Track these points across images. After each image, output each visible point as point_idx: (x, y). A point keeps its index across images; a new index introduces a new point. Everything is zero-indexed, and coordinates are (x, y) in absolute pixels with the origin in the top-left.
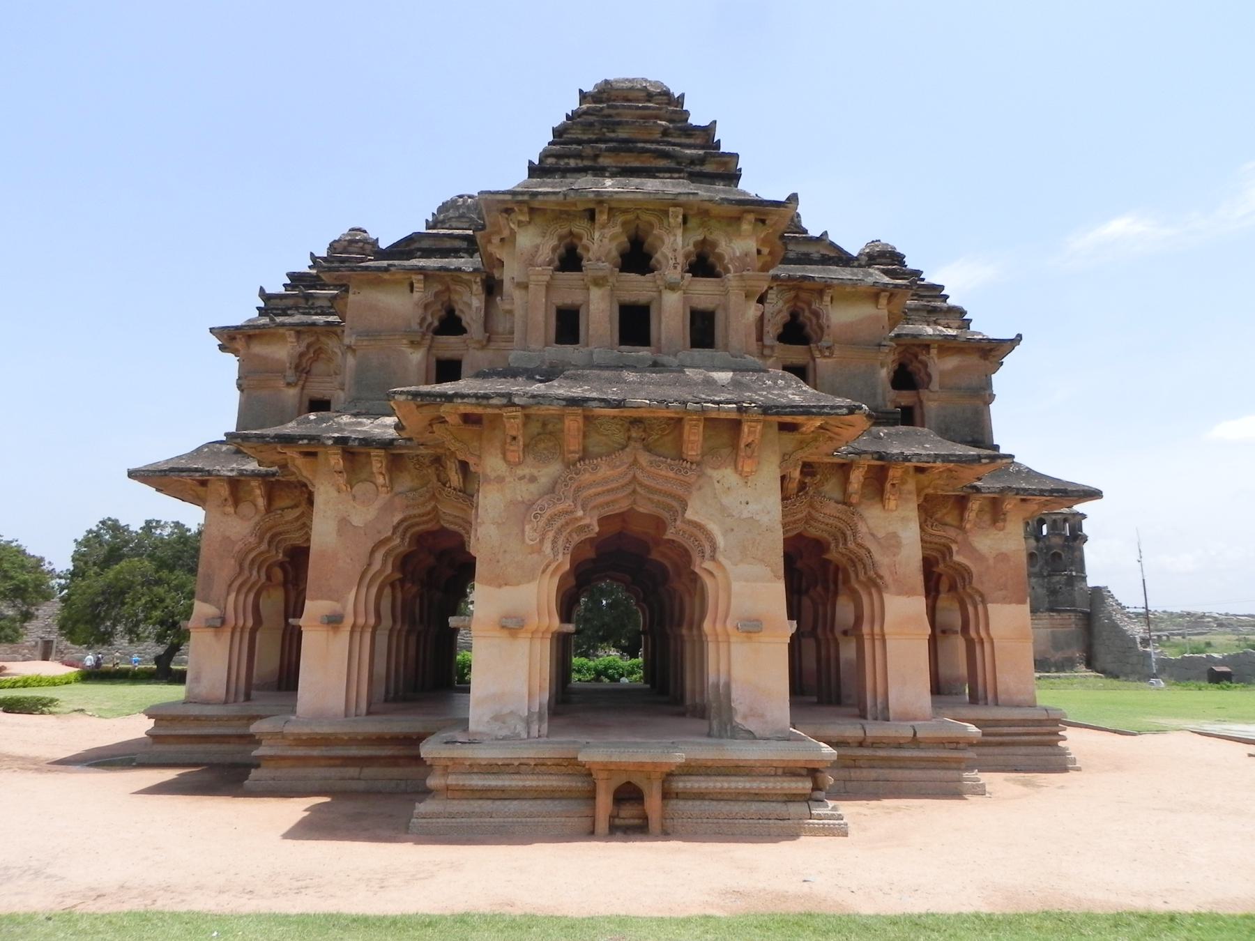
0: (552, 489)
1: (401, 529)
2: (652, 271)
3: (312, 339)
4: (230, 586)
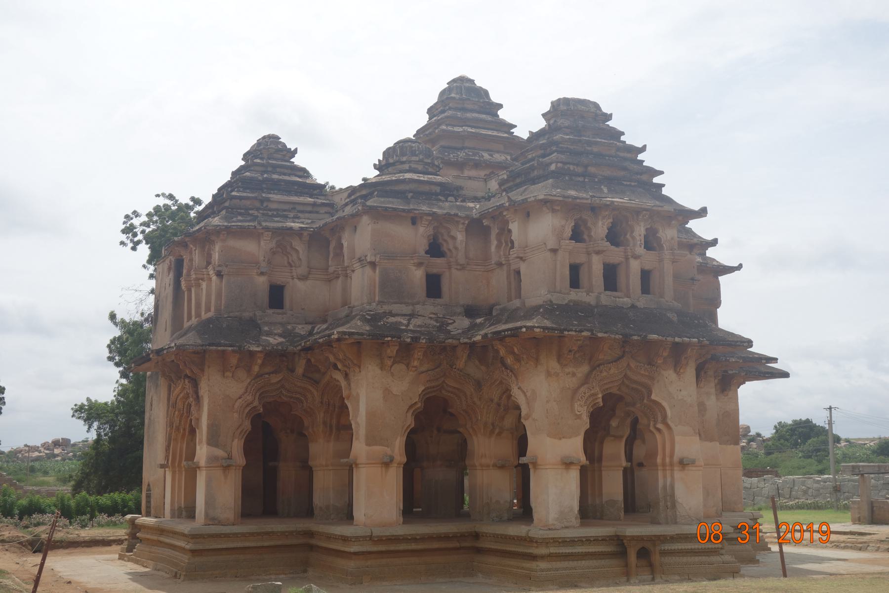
0: (586, 380)
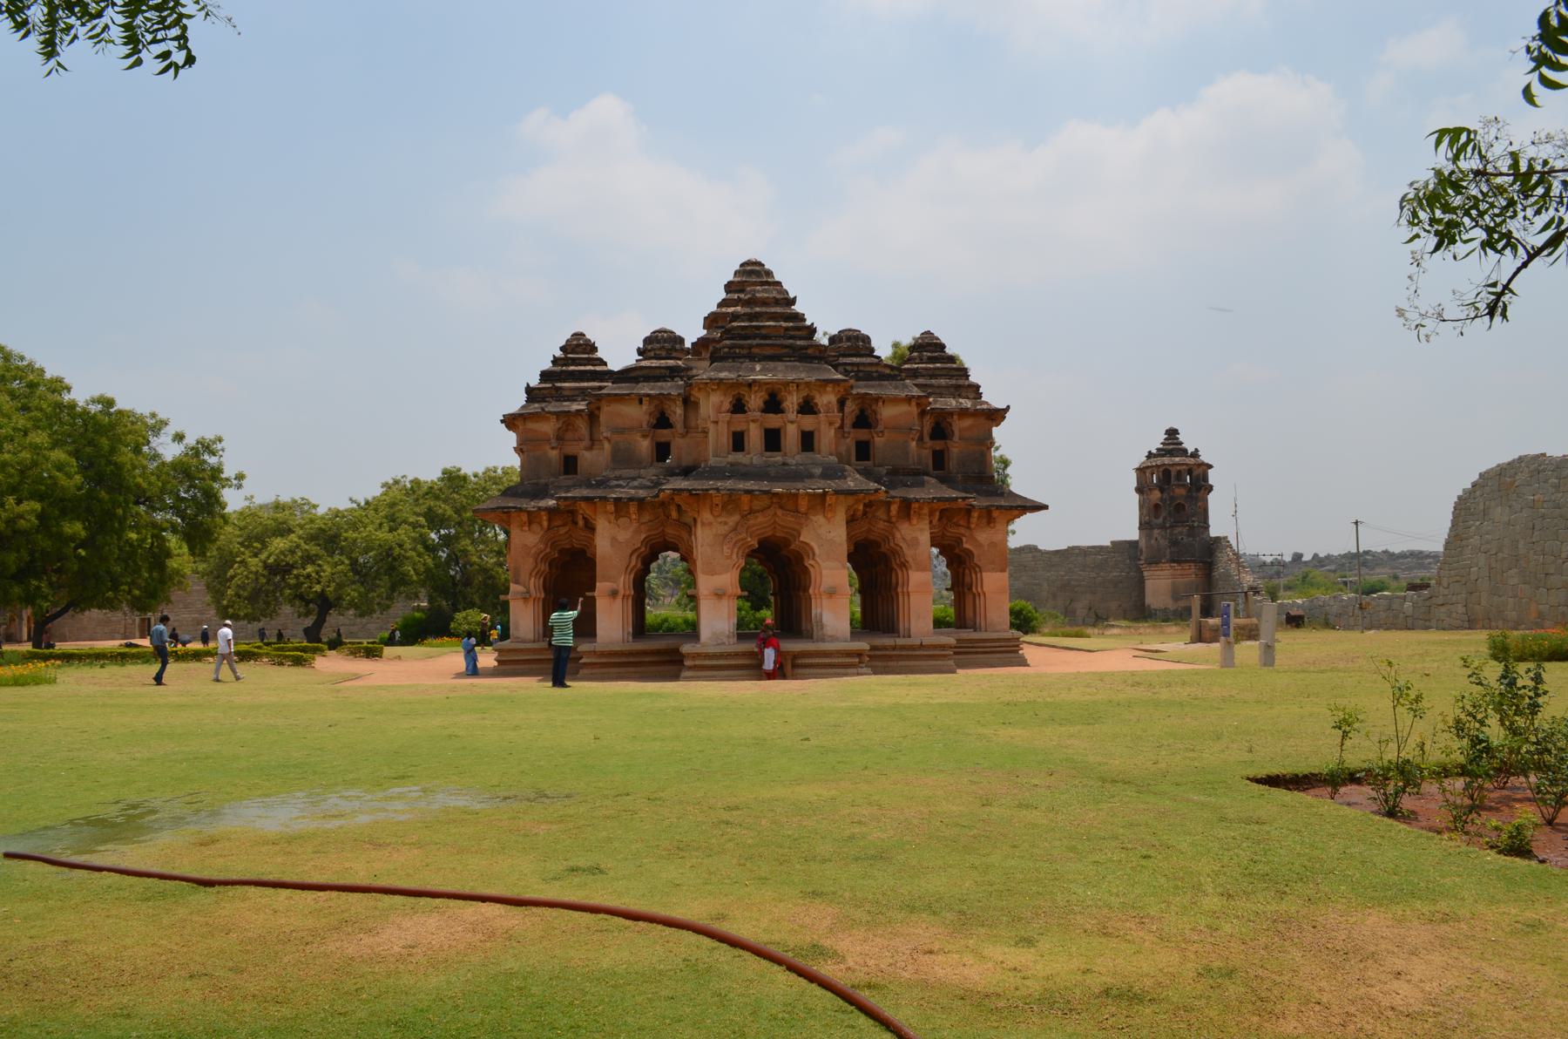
2: (782, 412)
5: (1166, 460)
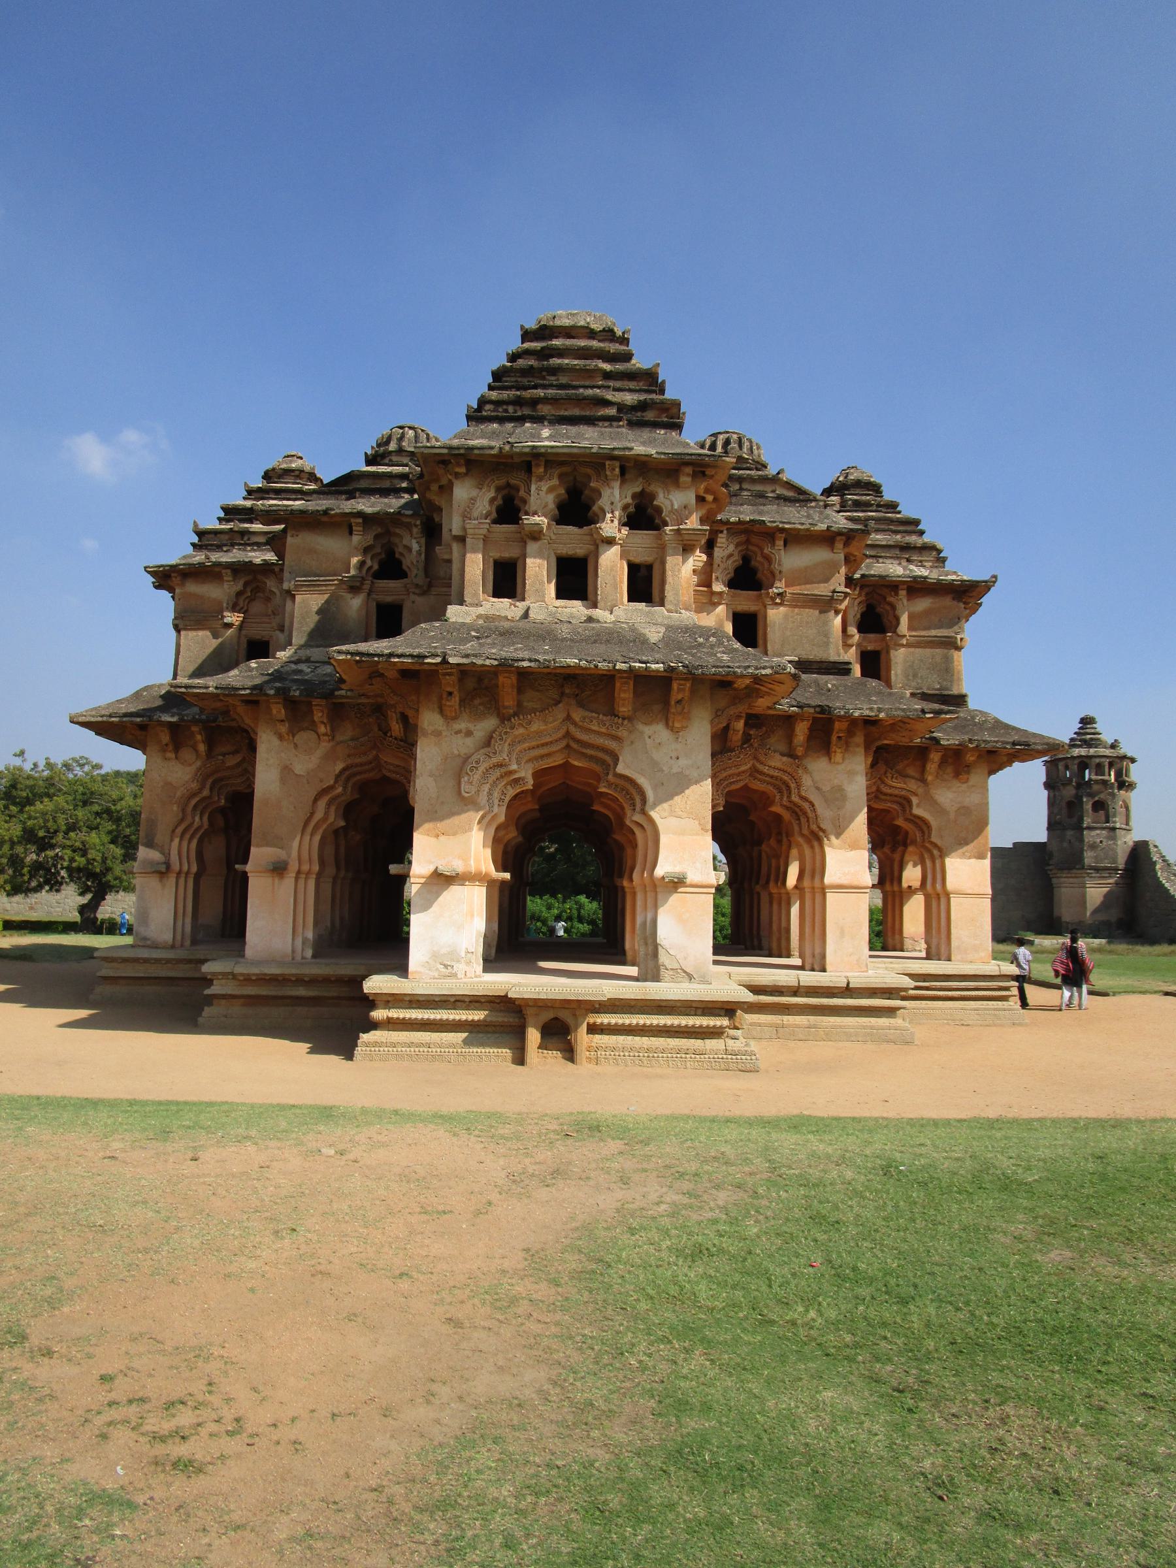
0: (488, 742)
1: (343, 777)
3: (250, 577)
4: (173, 831)
5: (1083, 751)
